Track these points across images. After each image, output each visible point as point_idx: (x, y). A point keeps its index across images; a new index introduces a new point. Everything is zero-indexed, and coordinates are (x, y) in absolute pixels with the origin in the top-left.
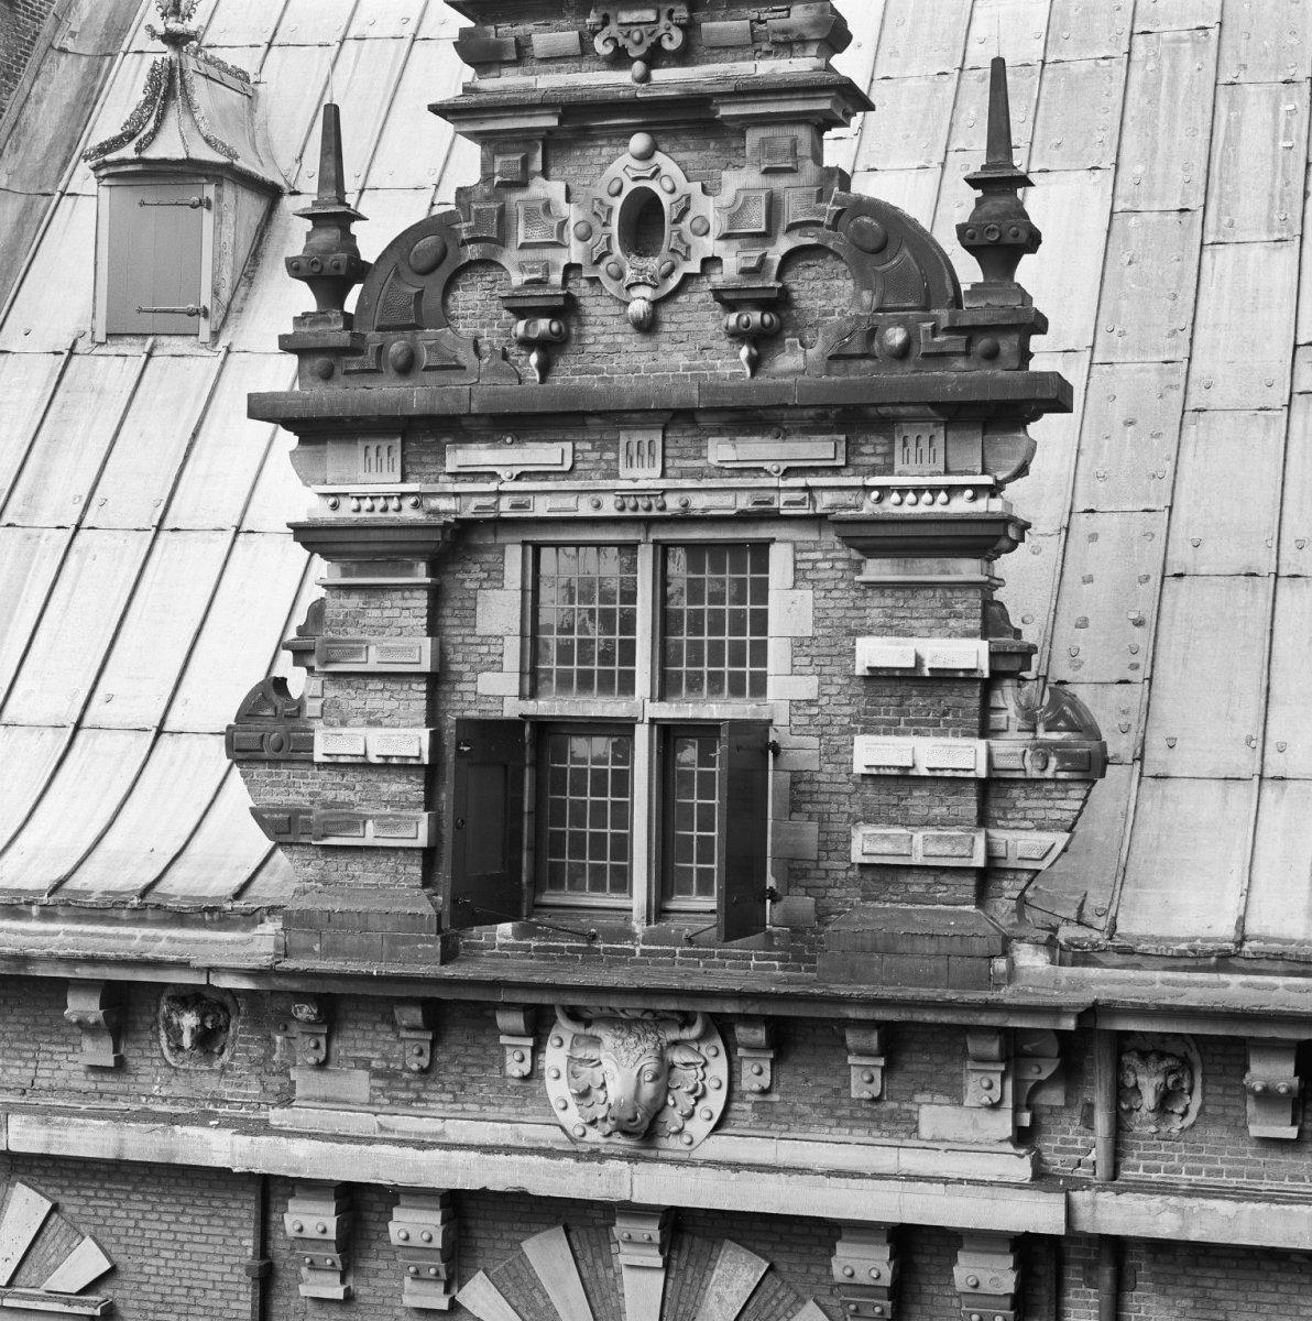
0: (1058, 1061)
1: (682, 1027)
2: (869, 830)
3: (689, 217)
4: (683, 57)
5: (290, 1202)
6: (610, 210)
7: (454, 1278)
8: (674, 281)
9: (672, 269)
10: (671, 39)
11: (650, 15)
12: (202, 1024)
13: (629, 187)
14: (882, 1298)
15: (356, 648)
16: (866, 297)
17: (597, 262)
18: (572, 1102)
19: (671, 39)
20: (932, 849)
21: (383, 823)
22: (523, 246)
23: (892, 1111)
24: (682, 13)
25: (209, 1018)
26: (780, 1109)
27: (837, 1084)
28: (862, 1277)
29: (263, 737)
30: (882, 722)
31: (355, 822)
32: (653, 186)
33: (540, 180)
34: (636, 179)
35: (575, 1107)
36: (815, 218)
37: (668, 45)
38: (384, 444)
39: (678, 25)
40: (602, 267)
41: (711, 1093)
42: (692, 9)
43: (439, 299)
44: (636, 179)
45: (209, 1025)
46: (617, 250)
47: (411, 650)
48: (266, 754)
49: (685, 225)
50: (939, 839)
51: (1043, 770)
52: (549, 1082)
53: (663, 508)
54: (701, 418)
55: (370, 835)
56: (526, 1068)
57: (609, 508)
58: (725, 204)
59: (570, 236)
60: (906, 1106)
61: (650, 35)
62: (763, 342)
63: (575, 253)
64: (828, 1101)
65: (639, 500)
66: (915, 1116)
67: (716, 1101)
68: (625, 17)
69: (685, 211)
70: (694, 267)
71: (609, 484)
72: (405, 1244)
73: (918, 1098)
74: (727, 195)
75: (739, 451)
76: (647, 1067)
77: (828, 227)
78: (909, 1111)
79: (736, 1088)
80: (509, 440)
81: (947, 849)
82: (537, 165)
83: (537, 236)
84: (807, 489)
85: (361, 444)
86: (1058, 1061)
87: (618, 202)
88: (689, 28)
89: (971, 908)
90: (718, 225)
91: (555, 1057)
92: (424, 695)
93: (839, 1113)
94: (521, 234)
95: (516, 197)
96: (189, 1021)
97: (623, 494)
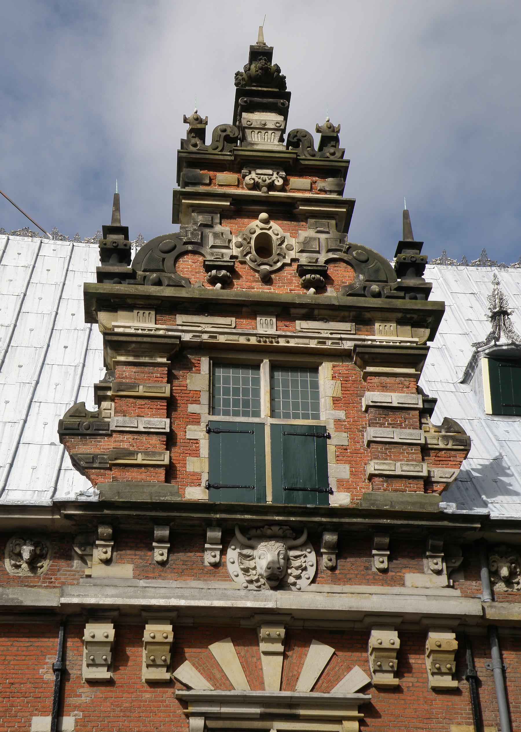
0: (463, 558)
1: (295, 539)
2: (376, 461)
3: (285, 244)
4: (283, 189)
5: (87, 624)
6: (251, 238)
7: (172, 667)
8: (279, 264)
9: (278, 261)
10: (278, 181)
11: (270, 172)
12: (34, 551)
13: (258, 232)
14: (393, 658)
15: (133, 386)
16: (361, 277)
17: (246, 255)
18: (241, 573)
19: (278, 181)
20: (405, 468)
21: (146, 453)
22: (213, 247)
23: (392, 576)
24: (283, 174)
25: (39, 548)
26: (340, 576)
27: (367, 564)
28: (386, 645)
29: (79, 423)
30: (378, 423)
31: (131, 454)
32: (270, 232)
33: (219, 226)
34: (261, 229)
35: (242, 575)
36: (339, 248)
37: (276, 183)
38: (147, 312)
39: (280, 177)
40: (248, 257)
41: (309, 568)
42: (287, 174)
43: (173, 262)
44: (261, 229)
45: (38, 552)
46: (254, 252)
47: (161, 387)
48: (81, 431)
49: (284, 246)
50: (408, 464)
51: (447, 445)
52: (229, 565)
53: (278, 342)
54: (293, 311)
55: (140, 459)
56: (217, 559)
57: (253, 341)
58: (300, 241)
59: (233, 245)
60: (398, 574)
61: (269, 179)
62: (320, 288)
63: (235, 251)
64: (363, 573)
65: (267, 340)
66: (403, 578)
67: (311, 572)
68: (259, 171)
69: (283, 242)
70: (288, 260)
71: (255, 332)
72: (152, 640)
73: (404, 571)
74: (301, 239)
75: (310, 325)
76: (281, 552)
77: (345, 252)
78: (400, 576)
79: (319, 568)
80: (206, 315)
81: (412, 468)
82: (218, 221)
83: (218, 243)
84: (341, 339)
85: (136, 312)
86: (463, 558)
87: (254, 236)
88: (286, 181)
89: (423, 493)
90: (297, 248)
91: (232, 554)
92: (166, 408)
93: (368, 577)
94: (211, 241)
95: (207, 230)
96: (26, 551)
97: (261, 336)
